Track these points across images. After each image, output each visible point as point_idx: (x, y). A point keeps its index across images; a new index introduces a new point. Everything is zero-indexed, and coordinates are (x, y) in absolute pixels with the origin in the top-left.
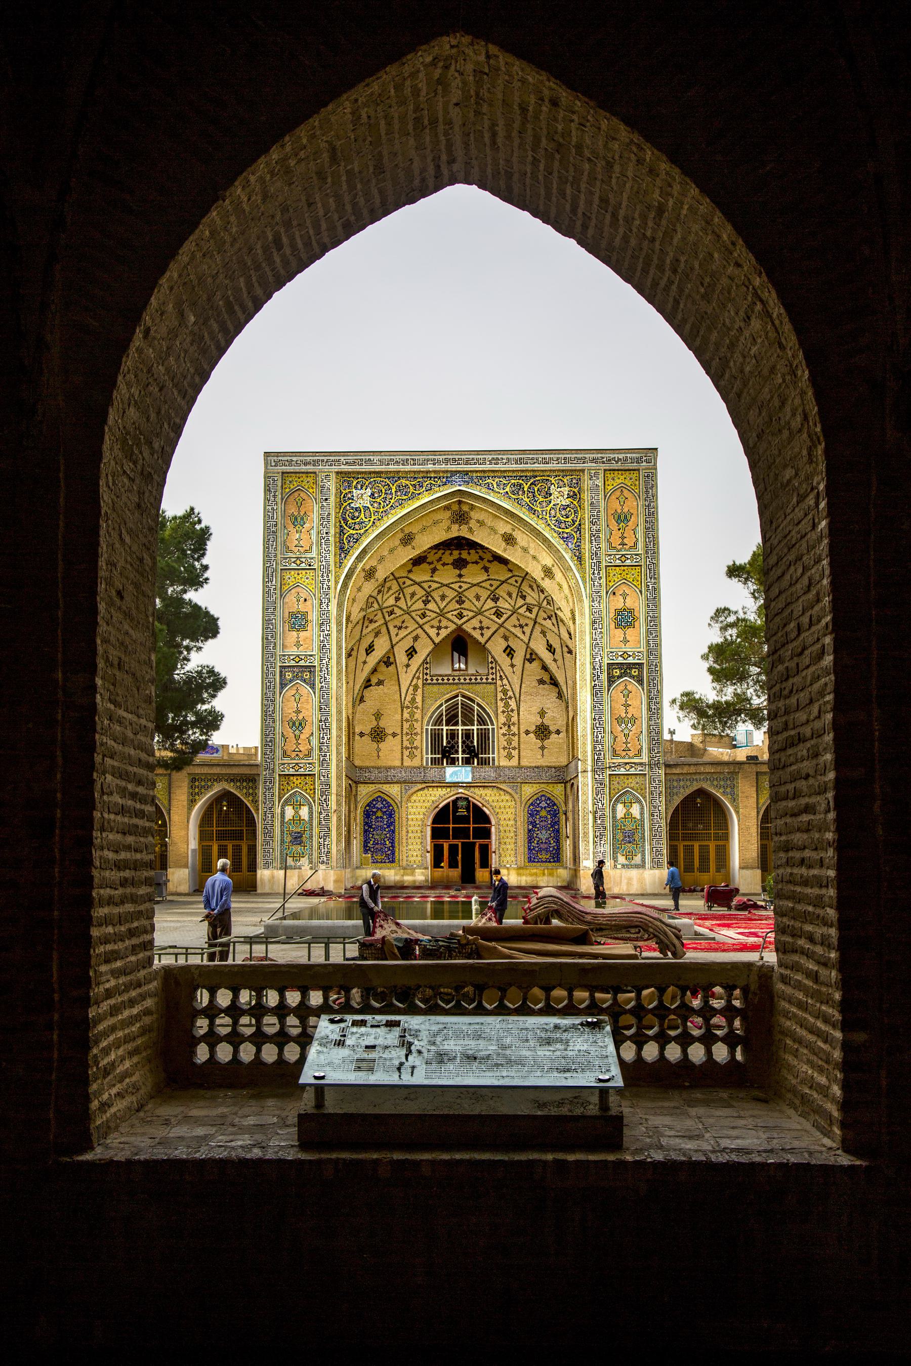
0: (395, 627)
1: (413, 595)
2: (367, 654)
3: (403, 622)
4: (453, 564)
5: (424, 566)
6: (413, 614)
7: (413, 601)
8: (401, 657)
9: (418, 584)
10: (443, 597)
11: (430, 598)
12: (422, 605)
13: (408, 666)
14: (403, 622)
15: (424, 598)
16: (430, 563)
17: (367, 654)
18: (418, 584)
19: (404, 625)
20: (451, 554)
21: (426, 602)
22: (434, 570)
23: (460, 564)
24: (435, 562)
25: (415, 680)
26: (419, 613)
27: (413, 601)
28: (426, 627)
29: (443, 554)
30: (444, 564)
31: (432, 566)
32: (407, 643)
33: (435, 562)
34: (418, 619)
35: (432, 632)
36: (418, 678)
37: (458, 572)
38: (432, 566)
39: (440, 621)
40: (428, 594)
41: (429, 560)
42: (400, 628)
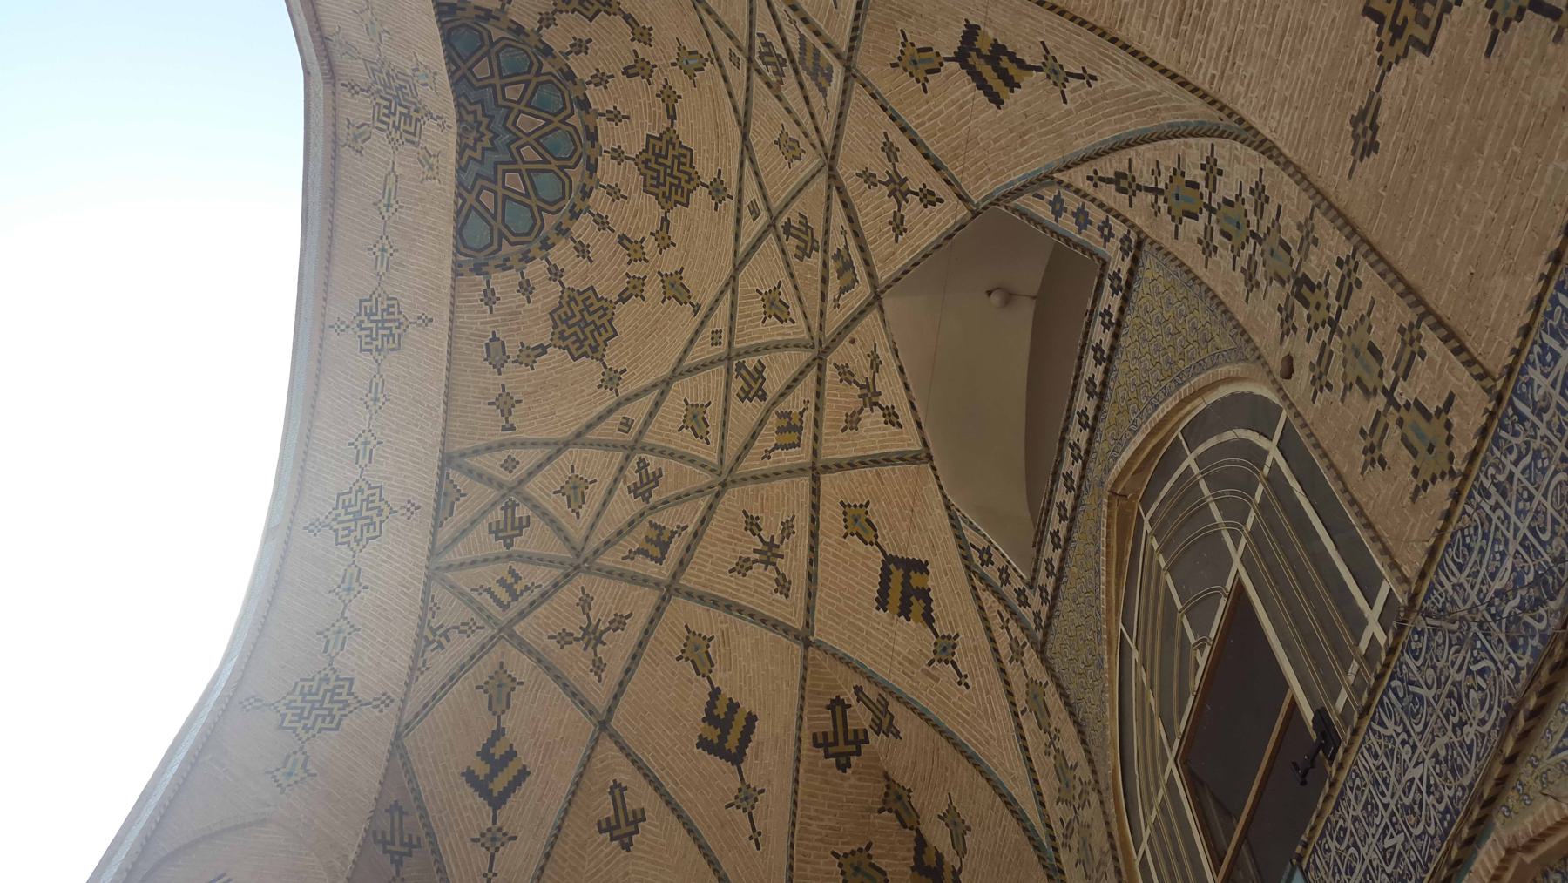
0: (743, 566)
1: (695, 419)
2: (737, 758)
3: (753, 524)
4: (666, 201)
5: (626, 317)
6: (752, 464)
7: (714, 434)
8: (890, 646)
9: (677, 374)
10: (775, 307)
11: (751, 362)
12: (754, 409)
13: (945, 649)
14: (753, 524)
15: (737, 384)
16: (633, 290)
17: (737, 758)
18: (677, 374)
19: (772, 529)
20: (614, 192)
21: (754, 387)
22: (675, 288)
23: (668, 171)
24: (638, 269)
25: (1013, 671)
26: (768, 437)
27: (714, 434)
28: (836, 447)
29: (602, 222)
30: (663, 236)
31: (653, 289)
32: (852, 571)
33: (638, 269)
34: (786, 458)
35: (874, 435)
36: (1017, 654)
37: (700, 196)
38: (653, 289)
39: (845, 374)
40: (731, 360)
41: (608, 288)
42: (770, 553)
